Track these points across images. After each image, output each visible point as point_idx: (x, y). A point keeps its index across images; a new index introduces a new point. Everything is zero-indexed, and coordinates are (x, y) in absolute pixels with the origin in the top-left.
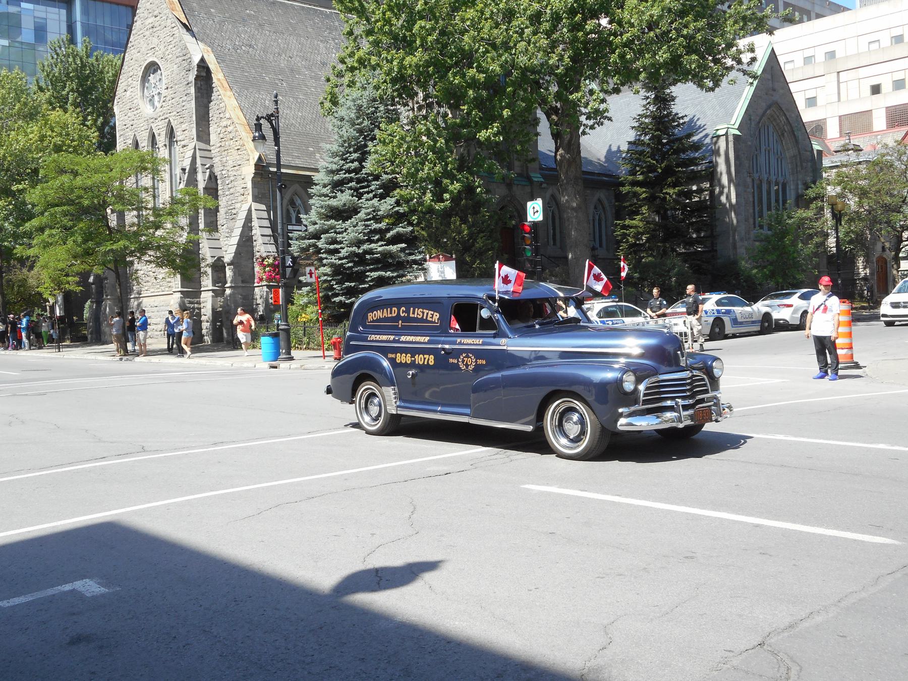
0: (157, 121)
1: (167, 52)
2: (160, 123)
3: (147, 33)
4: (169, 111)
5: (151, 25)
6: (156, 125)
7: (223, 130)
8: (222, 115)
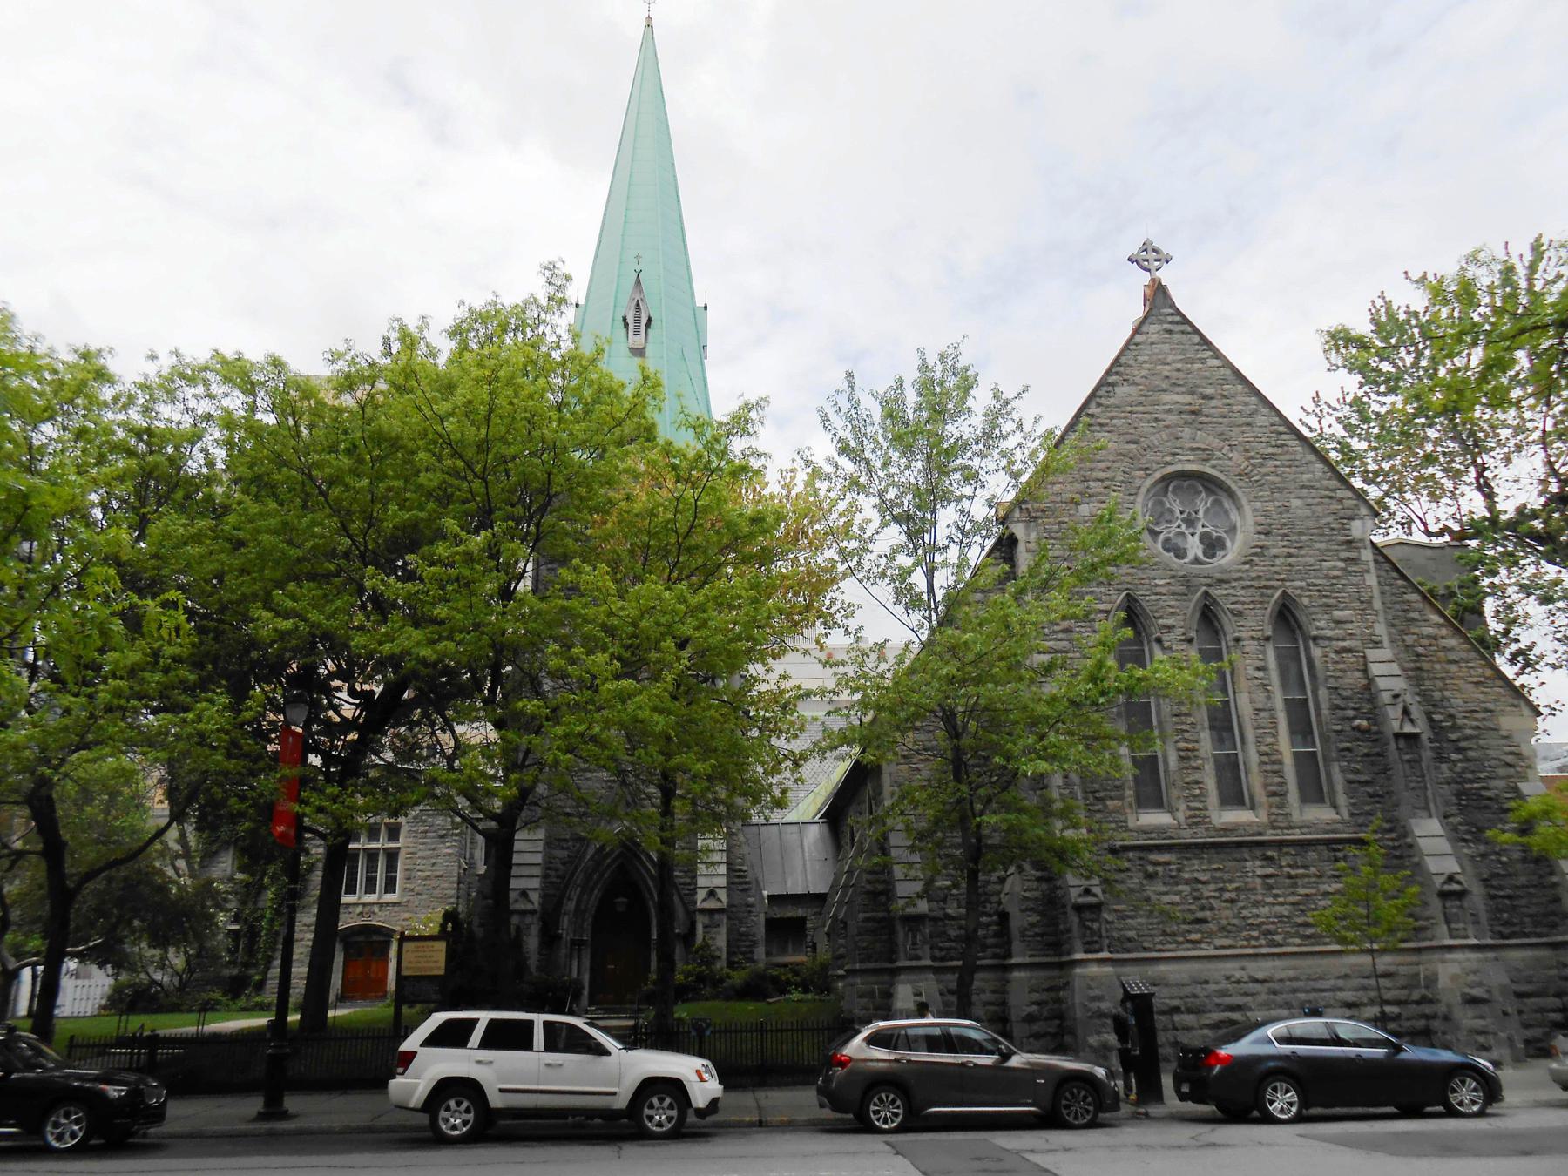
1: (1263, 470)
2: (1243, 592)
3: (1172, 419)
4: (1277, 577)
7: (1425, 642)
8: (1415, 615)
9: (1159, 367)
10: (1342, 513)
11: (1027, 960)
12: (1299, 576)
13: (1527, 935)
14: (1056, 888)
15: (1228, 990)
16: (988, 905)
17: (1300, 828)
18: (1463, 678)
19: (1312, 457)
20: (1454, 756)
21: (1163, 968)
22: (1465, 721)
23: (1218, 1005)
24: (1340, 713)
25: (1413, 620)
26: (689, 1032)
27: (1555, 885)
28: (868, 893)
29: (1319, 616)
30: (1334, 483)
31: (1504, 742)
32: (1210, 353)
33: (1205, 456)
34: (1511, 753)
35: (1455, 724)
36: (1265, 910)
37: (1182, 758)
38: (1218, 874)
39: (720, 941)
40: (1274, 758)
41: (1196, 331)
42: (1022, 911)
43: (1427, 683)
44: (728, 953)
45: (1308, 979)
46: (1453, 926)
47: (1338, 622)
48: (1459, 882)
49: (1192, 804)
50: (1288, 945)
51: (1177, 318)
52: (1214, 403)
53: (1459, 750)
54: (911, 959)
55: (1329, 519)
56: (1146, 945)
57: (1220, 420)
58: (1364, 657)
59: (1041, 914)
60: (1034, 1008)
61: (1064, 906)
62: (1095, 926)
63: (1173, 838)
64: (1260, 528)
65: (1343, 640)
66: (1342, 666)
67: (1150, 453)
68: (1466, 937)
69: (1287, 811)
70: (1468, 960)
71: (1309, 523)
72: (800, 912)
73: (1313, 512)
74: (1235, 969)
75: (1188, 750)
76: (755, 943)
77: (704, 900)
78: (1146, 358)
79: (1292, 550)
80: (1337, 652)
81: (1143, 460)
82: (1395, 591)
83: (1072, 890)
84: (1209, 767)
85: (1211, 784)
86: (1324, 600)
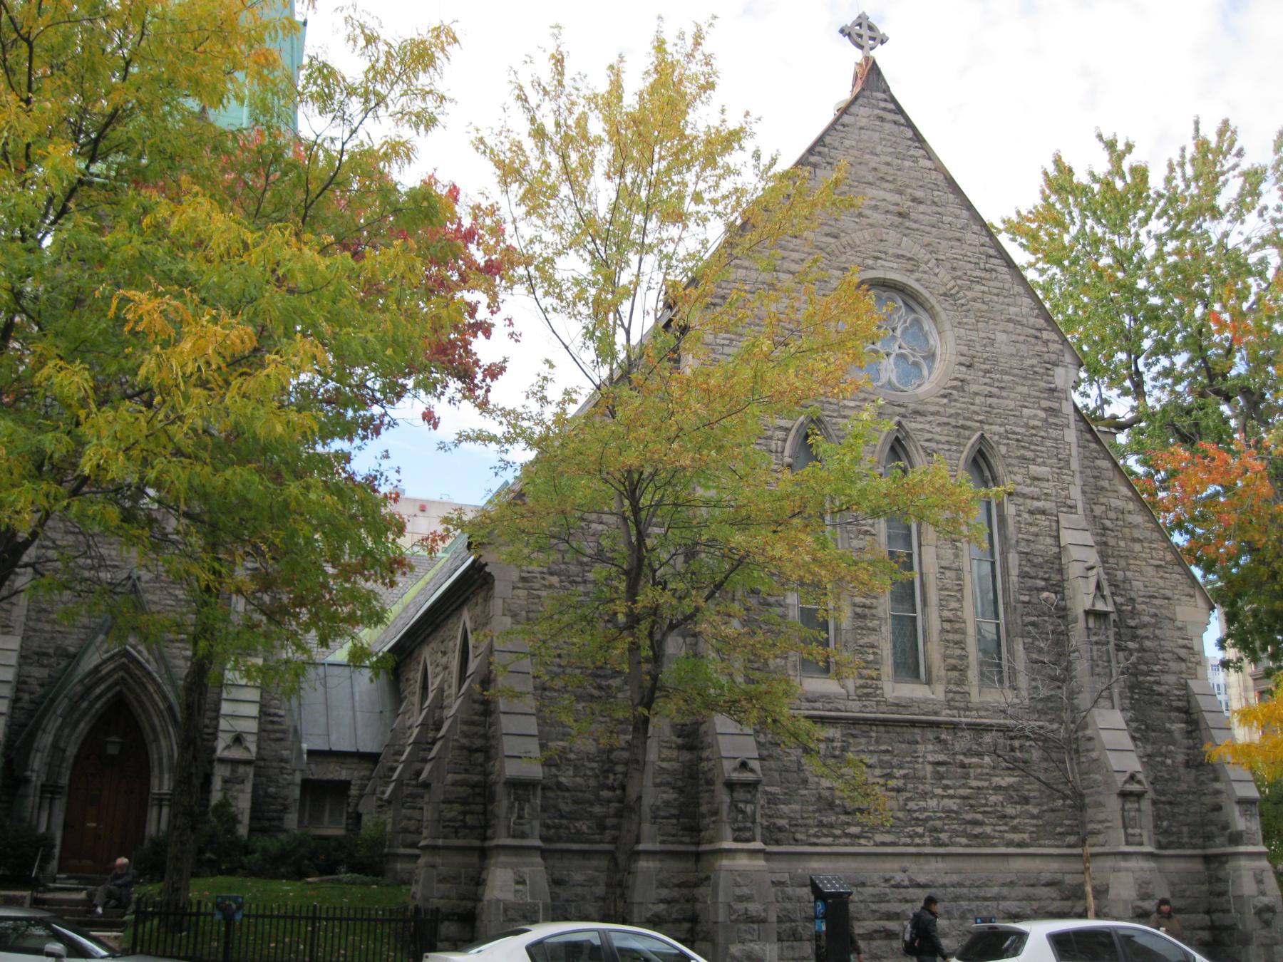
0: (919, 419)
1: (970, 294)
2: (938, 429)
3: (877, 217)
5: (901, 210)
6: (920, 426)
7: (1112, 515)
8: (1105, 484)
9: (867, 157)
10: (1046, 357)
11: (658, 847)
12: (998, 421)
13: (1182, 846)
14: (701, 759)
15: (886, 894)
16: (611, 776)
17: (977, 710)
18: (1145, 560)
19: (1018, 289)
20: (1131, 645)
21: (815, 864)
22: (1144, 607)
23: (874, 911)
24: (1030, 583)
25: (1103, 489)
26: (213, 915)
27: (1218, 792)
28: (462, 748)
29: (1016, 469)
30: (1041, 323)
31: (1178, 633)
32: (922, 152)
33: (909, 267)
34: (1185, 647)
35: (1134, 608)
36: (933, 803)
37: (858, 616)
38: (887, 758)
39: (243, 803)
40: (957, 626)
41: (910, 124)
42: (656, 785)
43: (1111, 560)
44: (252, 818)
45: (972, 886)
46: (1130, 831)
47: (1035, 479)
48: (1139, 782)
49: (865, 672)
50: (953, 844)
51: (891, 106)
52: (921, 208)
53: (1134, 638)
54: (514, 837)
55: (1034, 361)
56: (799, 836)
57: (928, 229)
58: (1058, 522)
59: (681, 791)
60: (662, 906)
61: (710, 782)
62: (749, 808)
63: (838, 710)
64: (962, 359)
65: (1038, 499)
66: (1034, 529)
67: (850, 252)
68: (1141, 844)
69: (966, 688)
70: (1142, 869)
71: (1015, 362)
72: (344, 775)
73: (1018, 351)
74: (895, 871)
75: (864, 606)
76: (285, 808)
77: (228, 747)
78: (854, 143)
79: (994, 390)
80: (1031, 512)
81: (843, 259)
82: (1087, 454)
83: (725, 762)
84: (886, 629)
85: (886, 649)
86: (1022, 452)
